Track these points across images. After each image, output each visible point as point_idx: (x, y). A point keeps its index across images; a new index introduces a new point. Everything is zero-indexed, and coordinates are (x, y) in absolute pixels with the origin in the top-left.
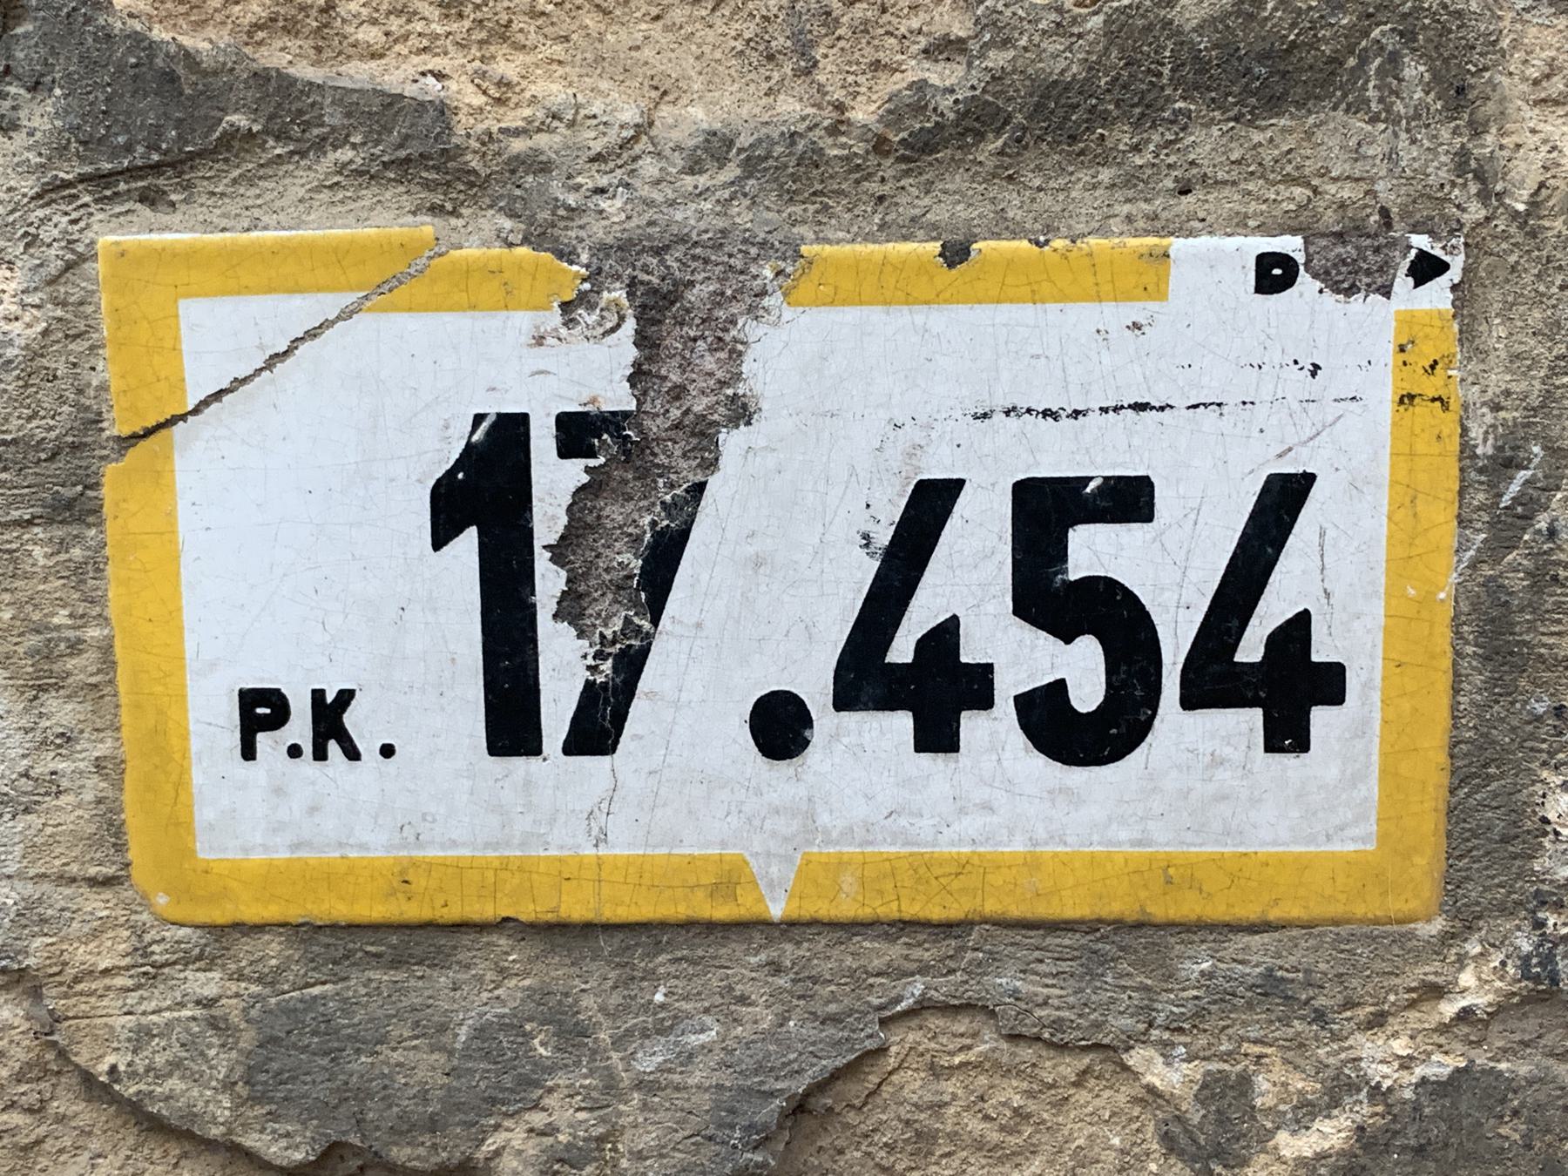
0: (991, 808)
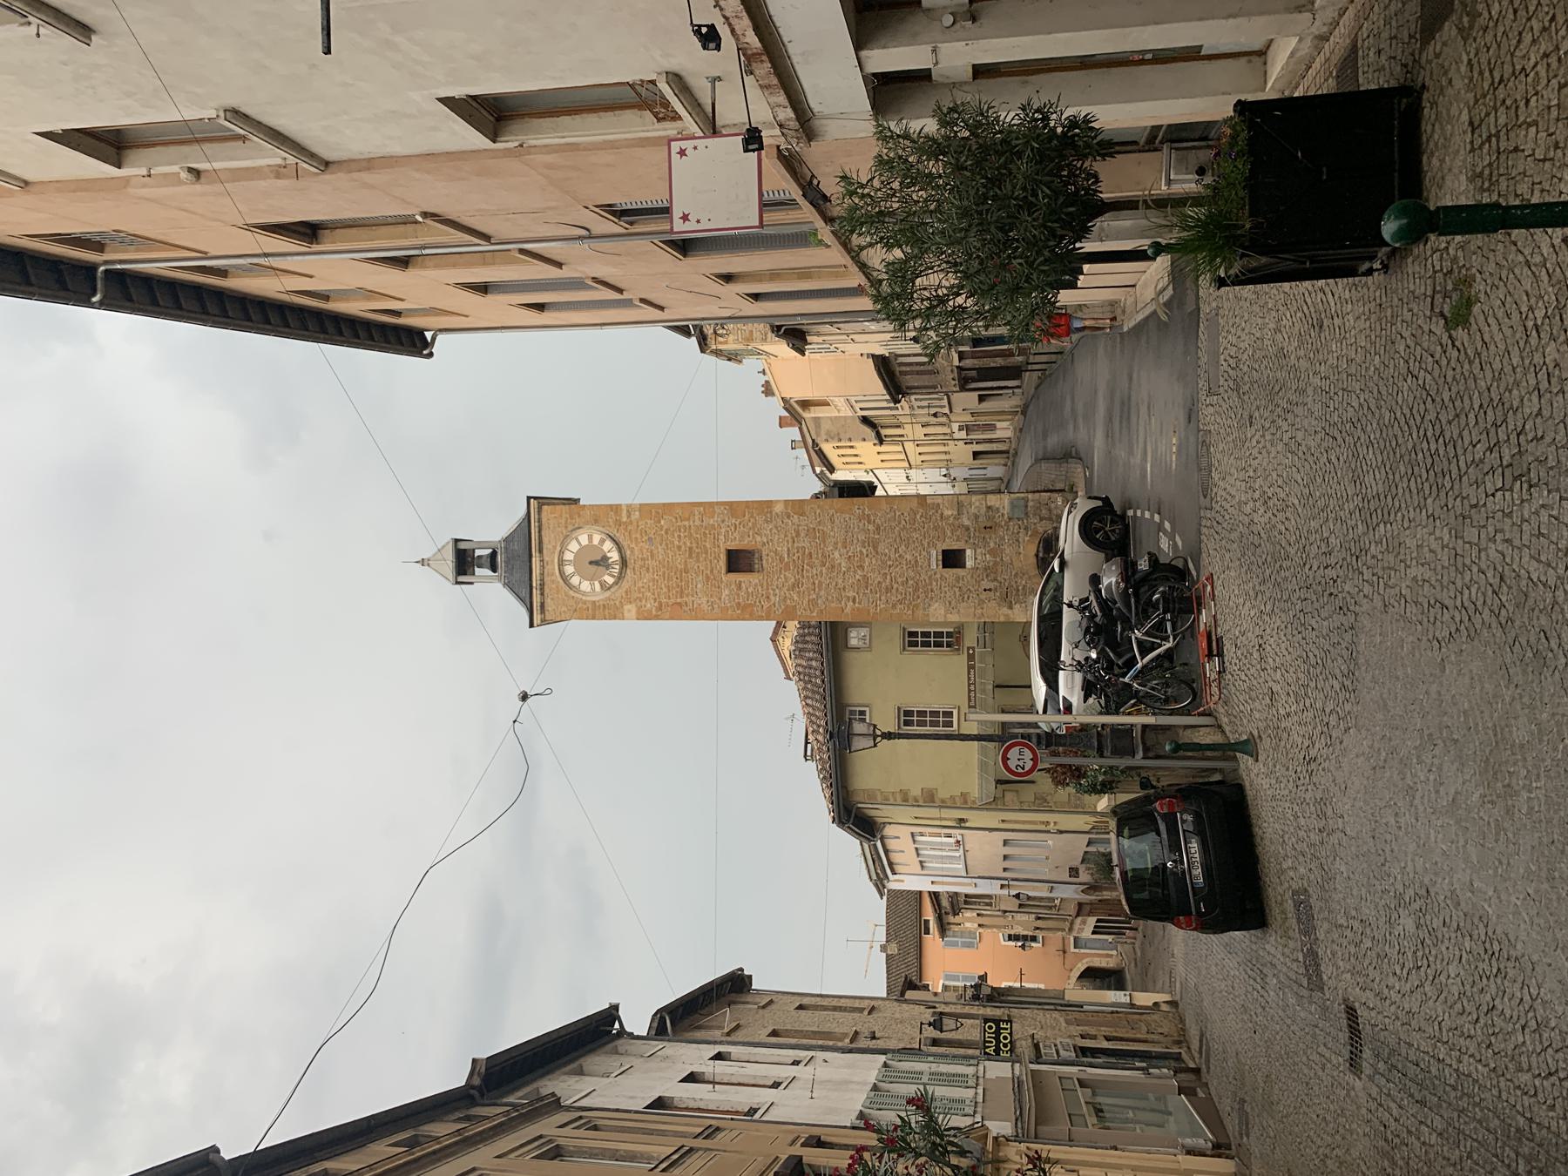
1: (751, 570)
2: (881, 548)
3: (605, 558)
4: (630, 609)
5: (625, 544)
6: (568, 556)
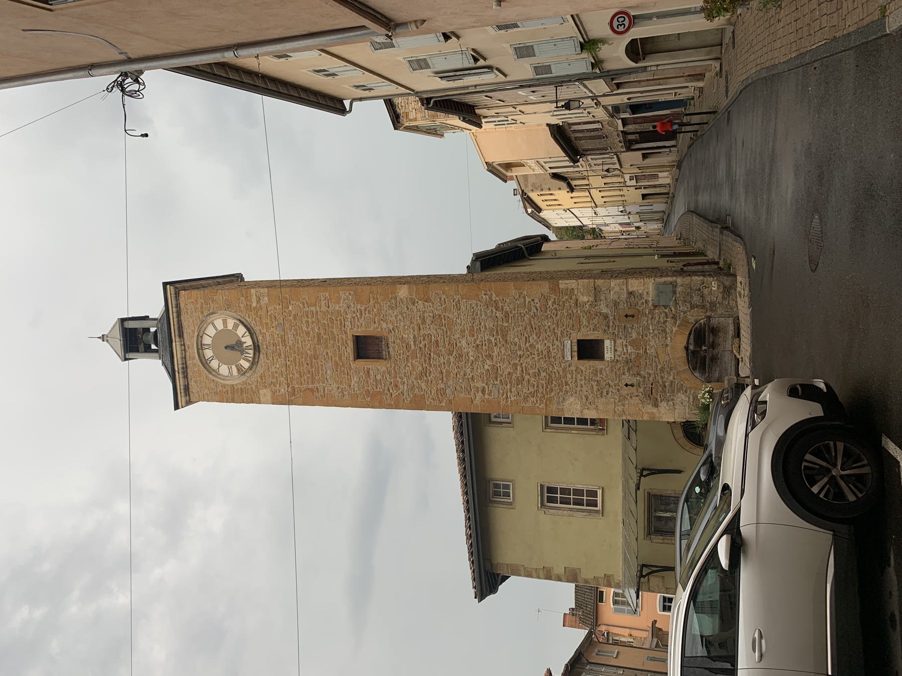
1: (379, 357)
2: (511, 337)
3: (240, 343)
4: (265, 392)
5: (257, 329)
6: (207, 340)
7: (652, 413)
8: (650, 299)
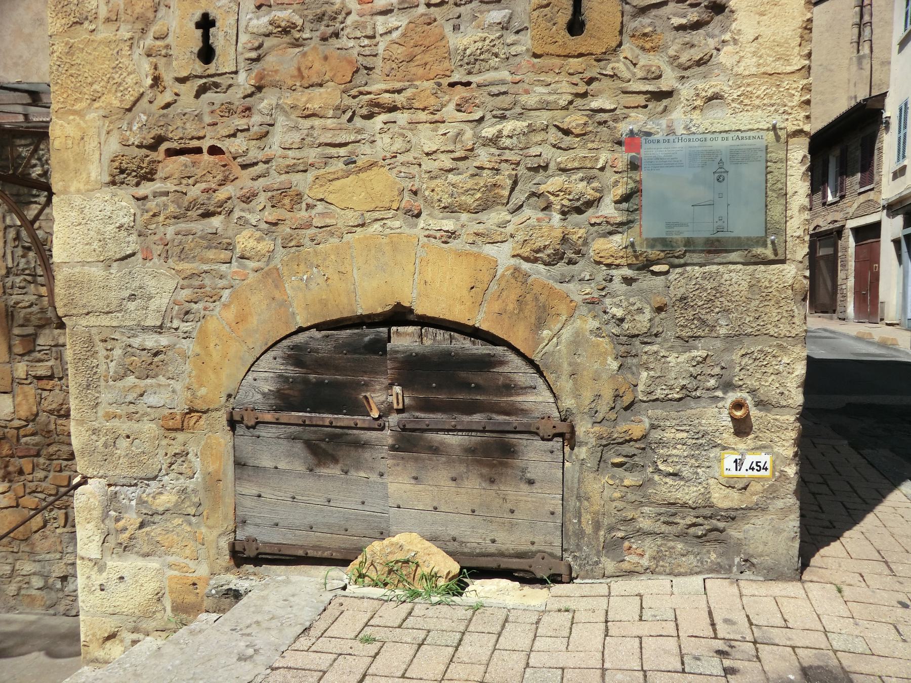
0: (755, 473)
7: (82, 158)
8: (678, 116)
